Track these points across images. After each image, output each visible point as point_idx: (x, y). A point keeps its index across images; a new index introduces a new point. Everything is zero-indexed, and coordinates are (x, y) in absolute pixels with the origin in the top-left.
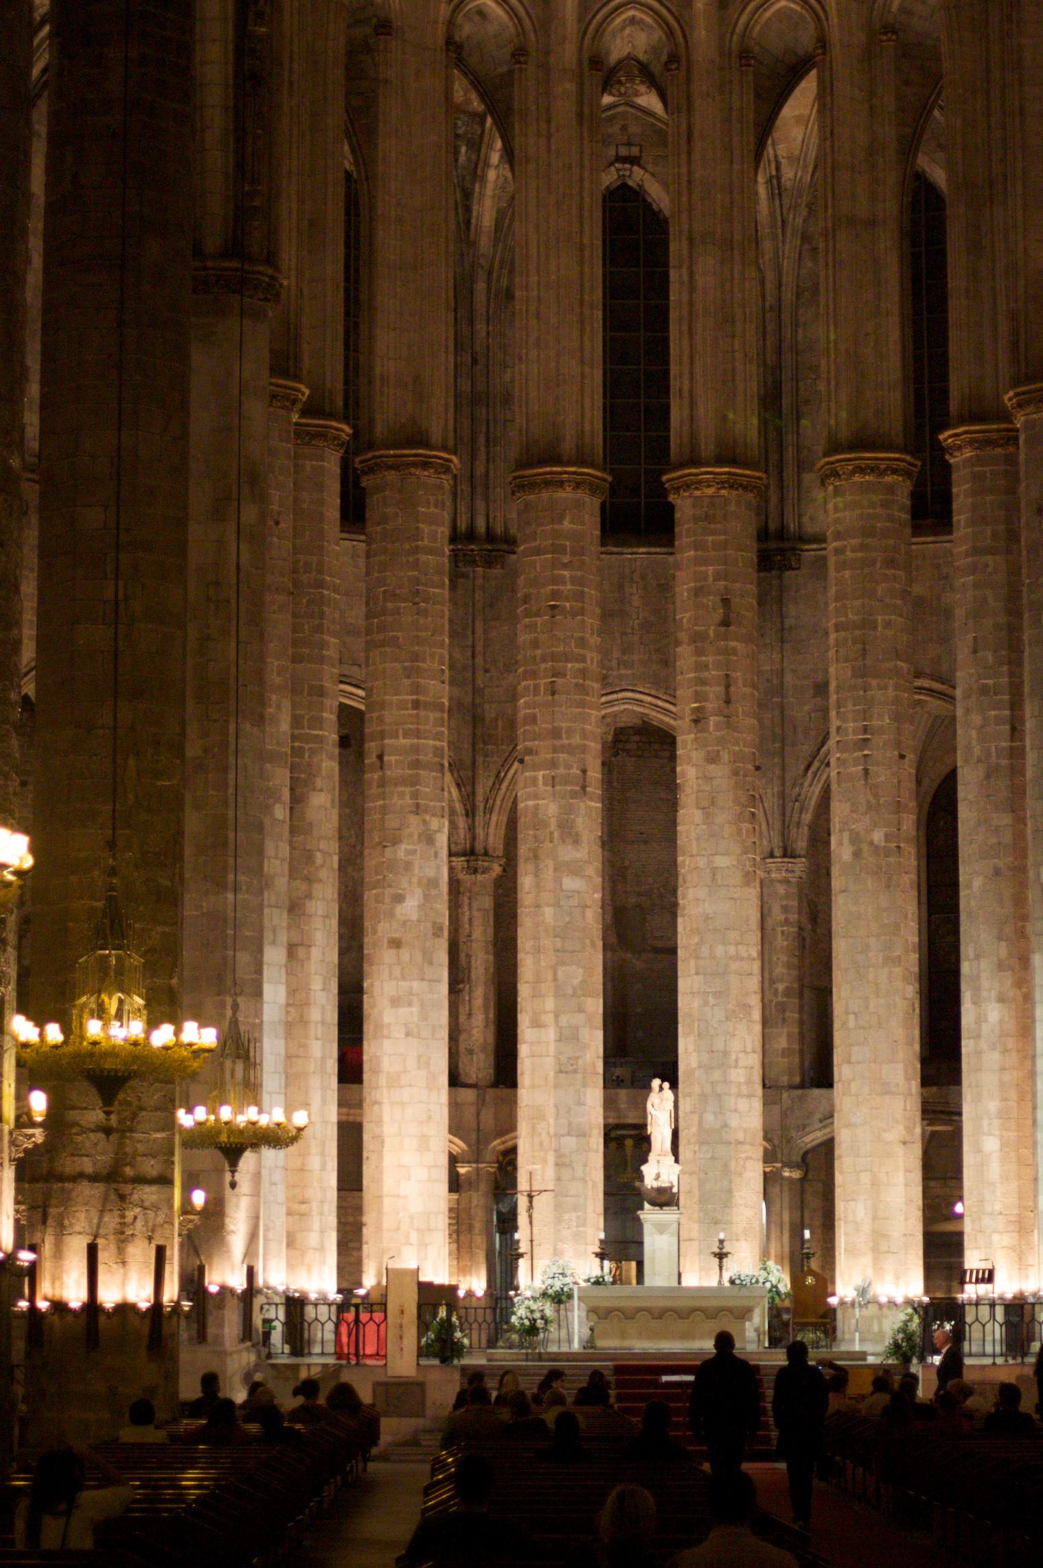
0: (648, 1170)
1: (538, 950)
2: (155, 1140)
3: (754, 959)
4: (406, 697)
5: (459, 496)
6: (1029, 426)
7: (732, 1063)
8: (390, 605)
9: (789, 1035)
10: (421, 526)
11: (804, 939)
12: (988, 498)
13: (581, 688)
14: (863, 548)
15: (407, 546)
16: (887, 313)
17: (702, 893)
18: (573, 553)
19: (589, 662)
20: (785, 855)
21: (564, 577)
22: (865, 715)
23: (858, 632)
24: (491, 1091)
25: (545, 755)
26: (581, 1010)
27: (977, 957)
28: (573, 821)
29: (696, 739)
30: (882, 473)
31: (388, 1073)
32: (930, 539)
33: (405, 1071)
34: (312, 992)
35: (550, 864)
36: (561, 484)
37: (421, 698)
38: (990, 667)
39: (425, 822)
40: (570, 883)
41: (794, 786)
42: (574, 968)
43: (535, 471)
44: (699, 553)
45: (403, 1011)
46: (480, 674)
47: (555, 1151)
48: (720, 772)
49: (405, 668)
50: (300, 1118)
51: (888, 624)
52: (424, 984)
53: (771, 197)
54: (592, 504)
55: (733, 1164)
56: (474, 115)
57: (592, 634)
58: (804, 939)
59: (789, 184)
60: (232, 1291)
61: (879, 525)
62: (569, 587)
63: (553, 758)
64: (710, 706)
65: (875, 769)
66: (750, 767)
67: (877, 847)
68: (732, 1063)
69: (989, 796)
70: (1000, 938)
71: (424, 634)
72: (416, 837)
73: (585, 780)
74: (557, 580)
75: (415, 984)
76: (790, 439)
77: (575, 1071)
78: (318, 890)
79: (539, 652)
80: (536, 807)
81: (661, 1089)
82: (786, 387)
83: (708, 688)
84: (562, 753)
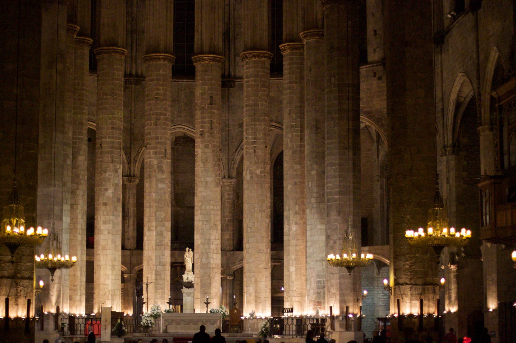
0: (185, 277)
1: (150, 207)
2: (28, 265)
3: (219, 210)
6: (308, 43)
7: (212, 243)
8: (104, 97)
11: (234, 204)
13: (165, 124)
14: (255, 81)
17: (202, 189)
19: (168, 115)
20: (229, 178)
22: (255, 133)
23: (253, 108)
24: (135, 252)
25: (153, 145)
26: (164, 226)
27: (289, 210)
28: (162, 166)
29: (201, 141)
30: (261, 57)
31: (102, 245)
32: (276, 78)
33: (108, 245)
34: (78, 220)
36: (159, 59)
37: (114, 126)
38: (294, 119)
39: (115, 166)
40: (161, 185)
41: (232, 156)
42: (162, 212)
44: (203, 82)
45: (107, 226)
46: (133, 119)
47: (155, 270)
48: (209, 151)
50: (74, 259)
51: (262, 105)
54: (169, 65)
55: (211, 275)
57: (169, 107)
60: (52, 314)
62: (162, 92)
64: (206, 130)
65: (258, 151)
66: (218, 149)
67: (258, 175)
70: (296, 204)
72: (112, 170)
73: (166, 153)
75: (111, 217)
77: (162, 245)
78: (80, 187)
79: (152, 112)
80: (150, 161)
81: (189, 251)
82: (232, 30)
84: (159, 144)
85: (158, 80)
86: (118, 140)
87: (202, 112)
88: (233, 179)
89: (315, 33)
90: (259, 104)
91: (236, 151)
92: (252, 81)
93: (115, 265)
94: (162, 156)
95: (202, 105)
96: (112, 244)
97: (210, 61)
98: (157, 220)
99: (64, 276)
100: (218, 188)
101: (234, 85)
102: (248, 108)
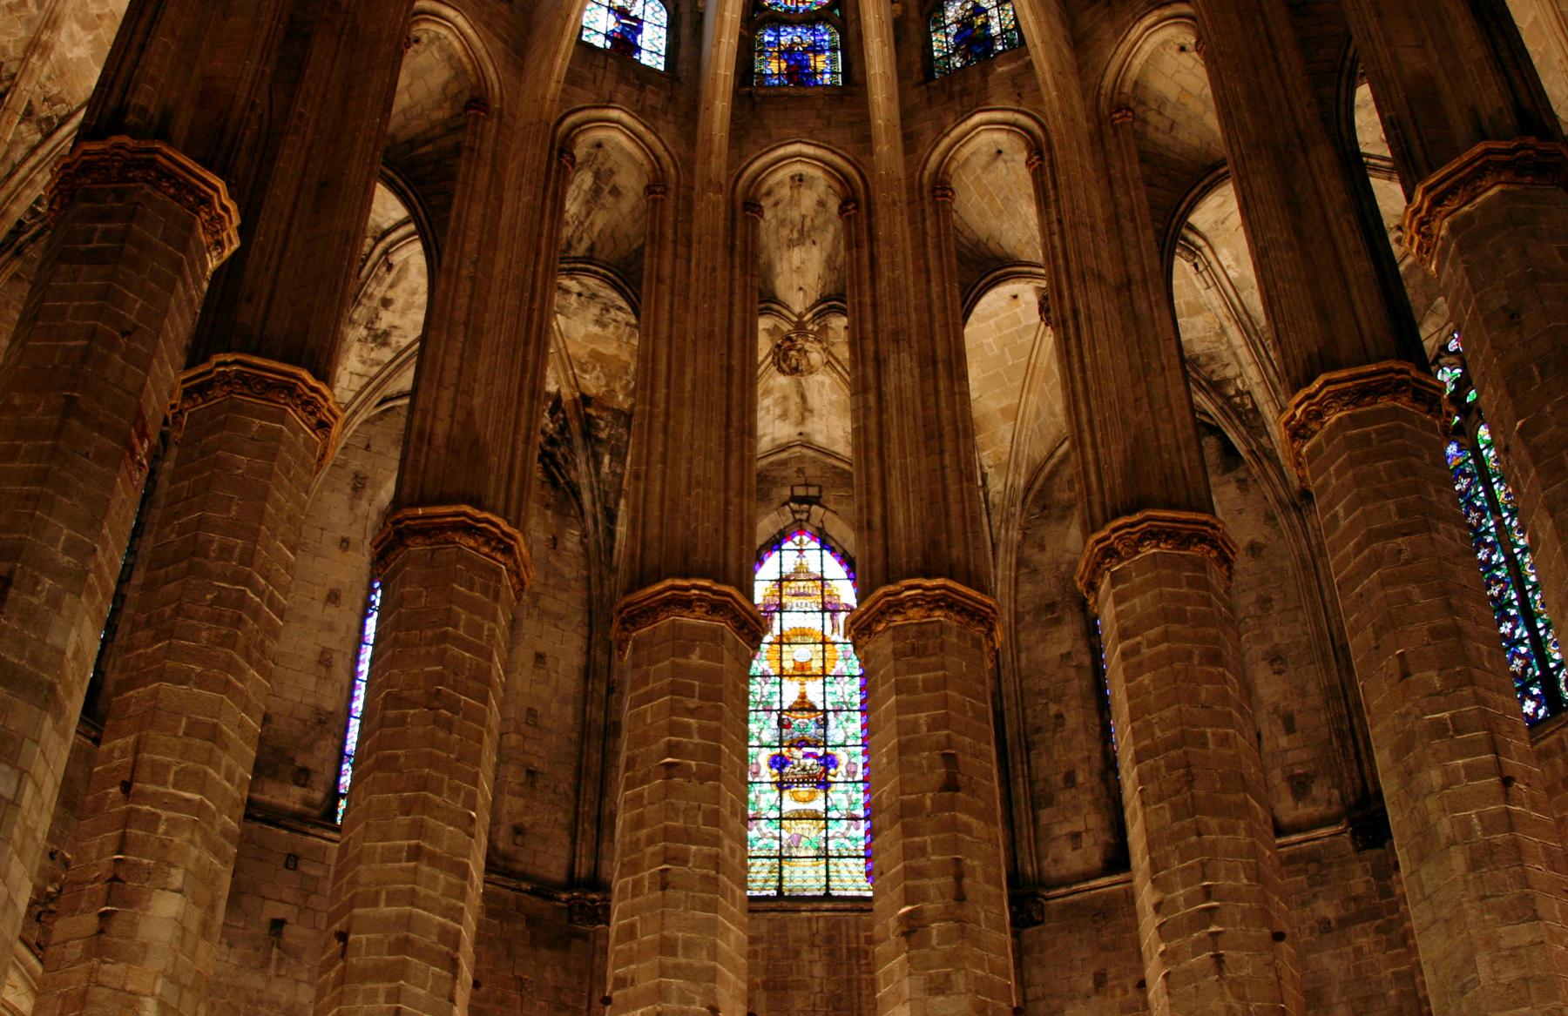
4: (398, 842)
5: (579, 838)
8: (391, 713)
10: (455, 607)
14: (1166, 637)
15: (429, 633)
16: (1163, 369)
18: (702, 697)
21: (688, 726)
29: (909, 960)
38: (1439, 694)
43: (650, 590)
44: (904, 697)
49: (403, 801)
51: (1224, 741)
56: (618, 413)
59: (997, 500)
61: (1189, 608)
62: (696, 740)
63: (659, 985)
69: (1484, 897)
74: (674, 729)
83: (926, 881)
84: (676, 977)
85: (674, 689)
87: (904, 826)
89: (1490, 157)
90: (1204, 734)
95: (905, 797)
97: (931, 610)
101: (1042, 912)
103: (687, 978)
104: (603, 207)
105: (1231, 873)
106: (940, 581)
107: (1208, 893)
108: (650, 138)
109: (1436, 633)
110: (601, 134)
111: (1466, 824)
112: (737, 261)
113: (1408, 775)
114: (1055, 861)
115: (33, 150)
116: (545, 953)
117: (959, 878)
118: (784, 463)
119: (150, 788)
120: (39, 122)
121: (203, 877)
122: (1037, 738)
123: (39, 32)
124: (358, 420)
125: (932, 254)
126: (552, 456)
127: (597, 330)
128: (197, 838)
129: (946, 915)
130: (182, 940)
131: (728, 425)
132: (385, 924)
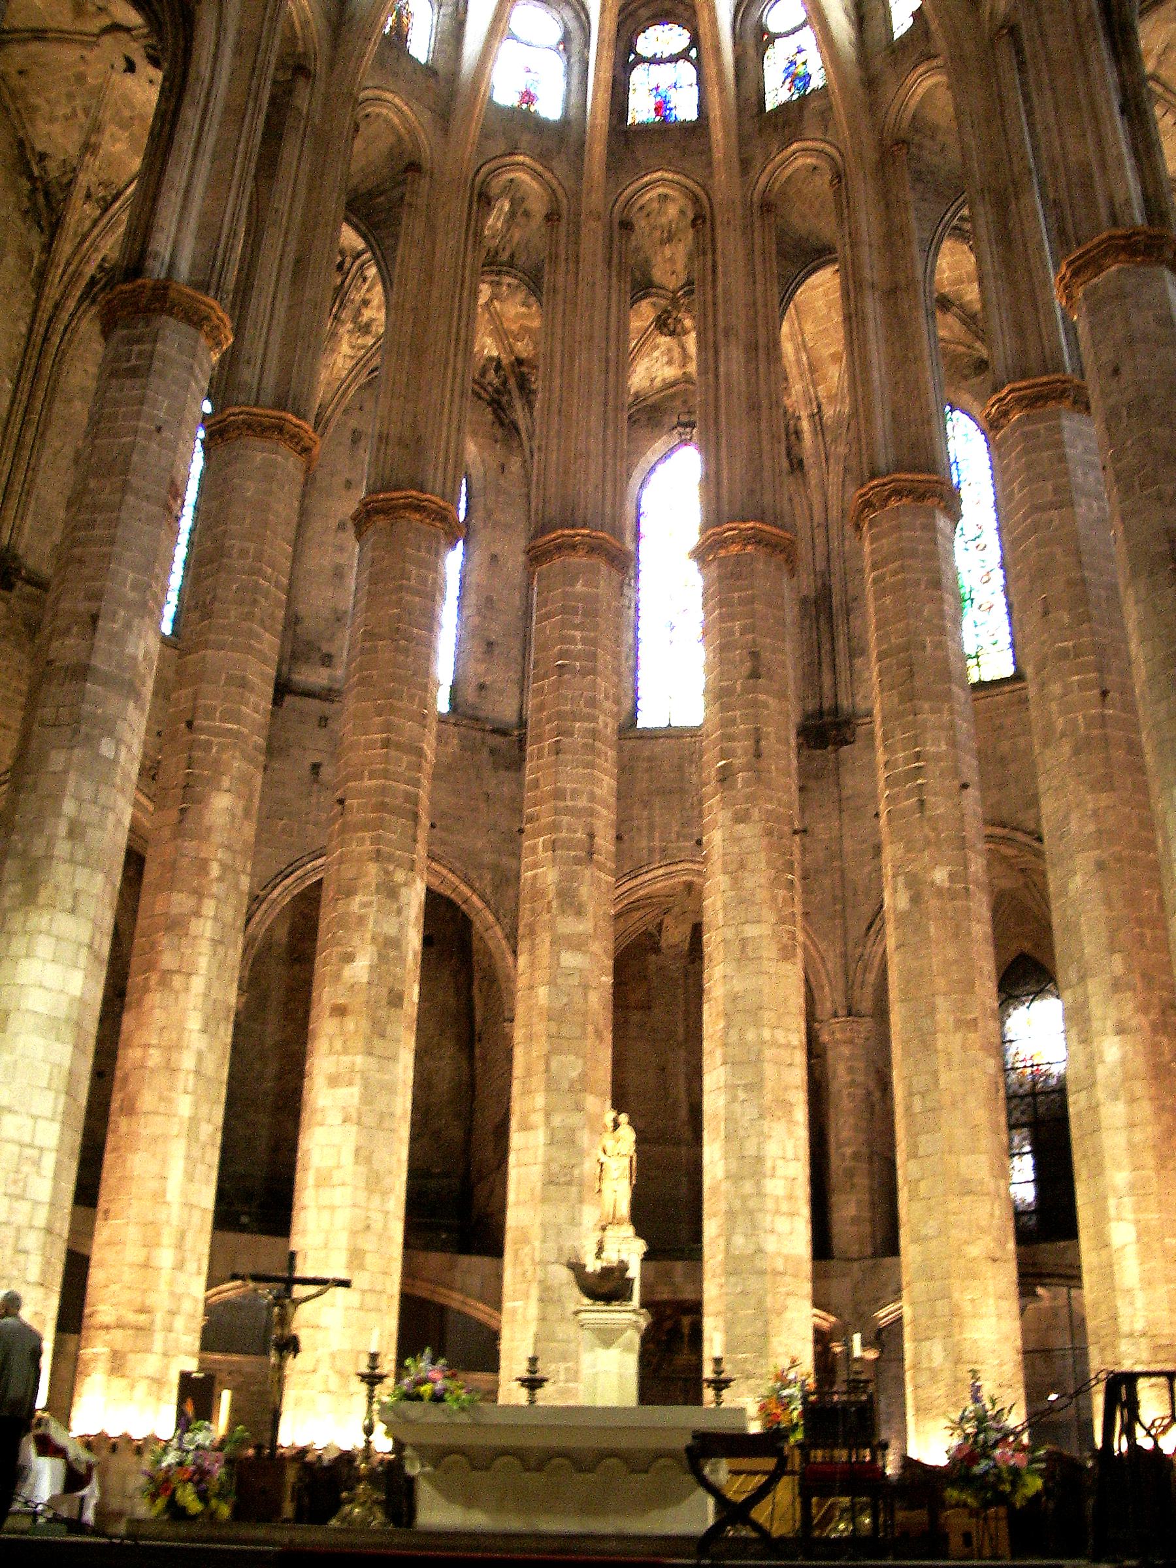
1: (530, 1037)
3: (795, 1048)
8: (368, 644)
9: (859, 1202)
11: (872, 1106)
12: (1045, 454)
13: (592, 749)
14: (902, 569)
19: (601, 724)
20: (849, 1015)
21: (574, 637)
22: (916, 741)
25: (544, 821)
26: (579, 1108)
29: (722, 799)
33: (339, 1167)
34: (187, 1034)
35: (545, 938)
36: (574, 547)
39: (387, 873)
40: (569, 959)
41: (856, 945)
42: (572, 1058)
43: (547, 538)
48: (749, 832)
52: (372, 1062)
53: (815, 432)
58: (872, 1106)
68: (769, 1173)
70: (1112, 950)
71: (402, 672)
74: (564, 640)
75: (359, 1060)
76: (841, 630)
77: (569, 1183)
80: (535, 877)
81: (616, 1125)
82: (836, 589)
83: (736, 744)
85: (564, 610)
86: (403, 786)
88: (861, 1020)
91: (869, 927)
92: (895, 573)
93: (365, 1252)
94: (575, 857)
96: (356, 1163)
98: (551, 1086)
99: (18, 1230)
100: (788, 966)
102: (887, 661)
103: (572, 815)
104: (518, 225)
105: (935, 741)
106: (751, 524)
107: (918, 757)
108: (548, 175)
109: (1070, 583)
110: (511, 175)
111: (1074, 722)
112: (614, 273)
113: (1043, 685)
114: (865, 697)
115: (95, 223)
116: (502, 773)
117: (758, 741)
118: (673, 397)
119: (206, 723)
120: (97, 201)
121: (246, 780)
122: (855, 604)
123: (88, 136)
124: (352, 391)
125: (758, 260)
126: (499, 403)
127: (524, 309)
128: (237, 754)
129: (748, 768)
130: (233, 822)
131: (606, 404)
132: (368, 793)
